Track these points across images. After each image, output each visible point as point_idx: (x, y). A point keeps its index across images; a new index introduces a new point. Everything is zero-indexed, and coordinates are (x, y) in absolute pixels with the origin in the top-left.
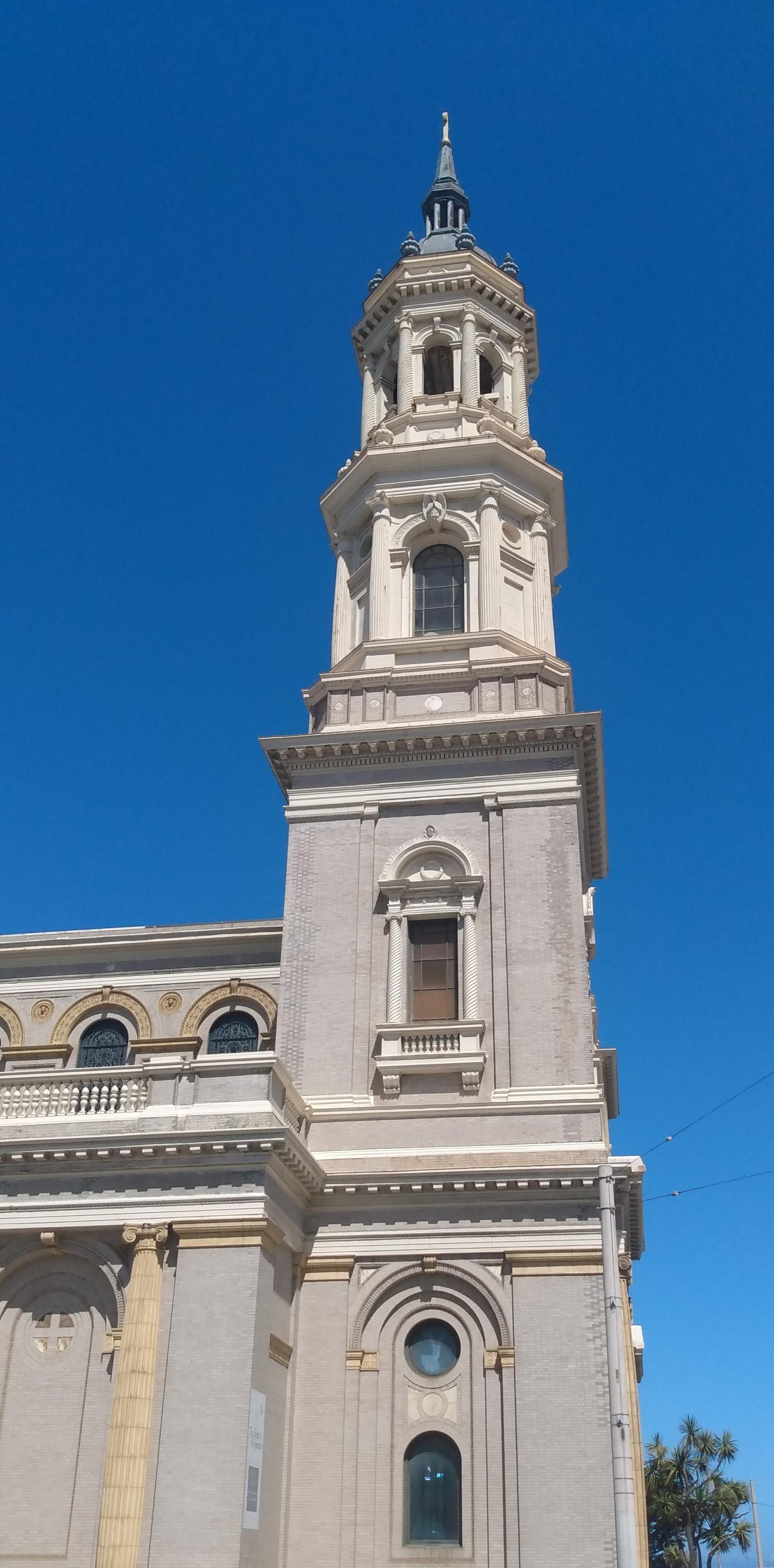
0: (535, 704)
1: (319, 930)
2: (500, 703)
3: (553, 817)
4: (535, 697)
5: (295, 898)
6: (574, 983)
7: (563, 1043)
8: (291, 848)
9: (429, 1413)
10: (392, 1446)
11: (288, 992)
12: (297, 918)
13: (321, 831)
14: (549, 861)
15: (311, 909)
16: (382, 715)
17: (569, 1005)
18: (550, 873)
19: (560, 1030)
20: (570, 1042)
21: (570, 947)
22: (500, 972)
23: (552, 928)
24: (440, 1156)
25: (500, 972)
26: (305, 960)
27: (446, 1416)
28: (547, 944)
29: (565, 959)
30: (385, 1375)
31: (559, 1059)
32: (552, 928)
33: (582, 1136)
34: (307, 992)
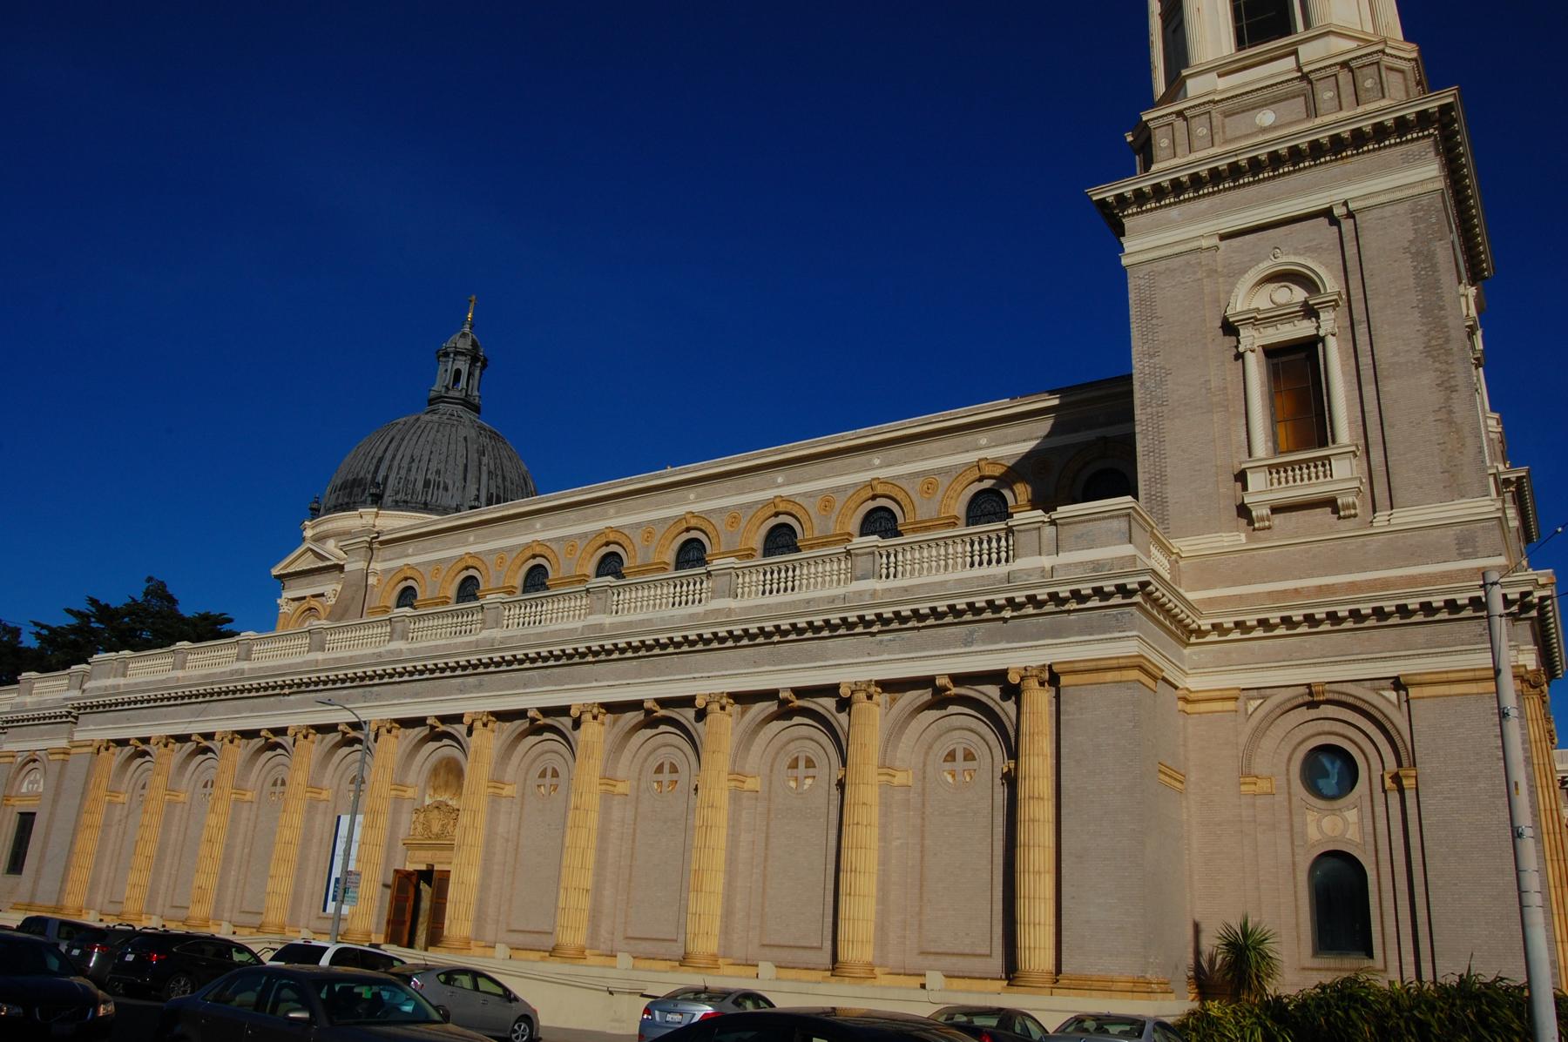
0: (1380, 95)
1: (1170, 374)
2: (1340, 102)
3: (1413, 215)
4: (1379, 86)
6: (1456, 391)
7: (1450, 456)
8: (1132, 296)
9: (1330, 834)
10: (1294, 864)
11: (1145, 440)
13: (1160, 273)
14: (1415, 263)
16: (1210, 143)
17: (1453, 415)
18: (1417, 276)
19: (1444, 443)
20: (1457, 454)
21: (1448, 352)
22: (1369, 391)
23: (1426, 335)
24: (1320, 586)
25: (1369, 391)
26: (1159, 406)
27: (1347, 836)
28: (1421, 353)
29: (1444, 367)
30: (1281, 798)
31: (1446, 474)
32: (1426, 335)
33: (1478, 552)
34: (1164, 437)
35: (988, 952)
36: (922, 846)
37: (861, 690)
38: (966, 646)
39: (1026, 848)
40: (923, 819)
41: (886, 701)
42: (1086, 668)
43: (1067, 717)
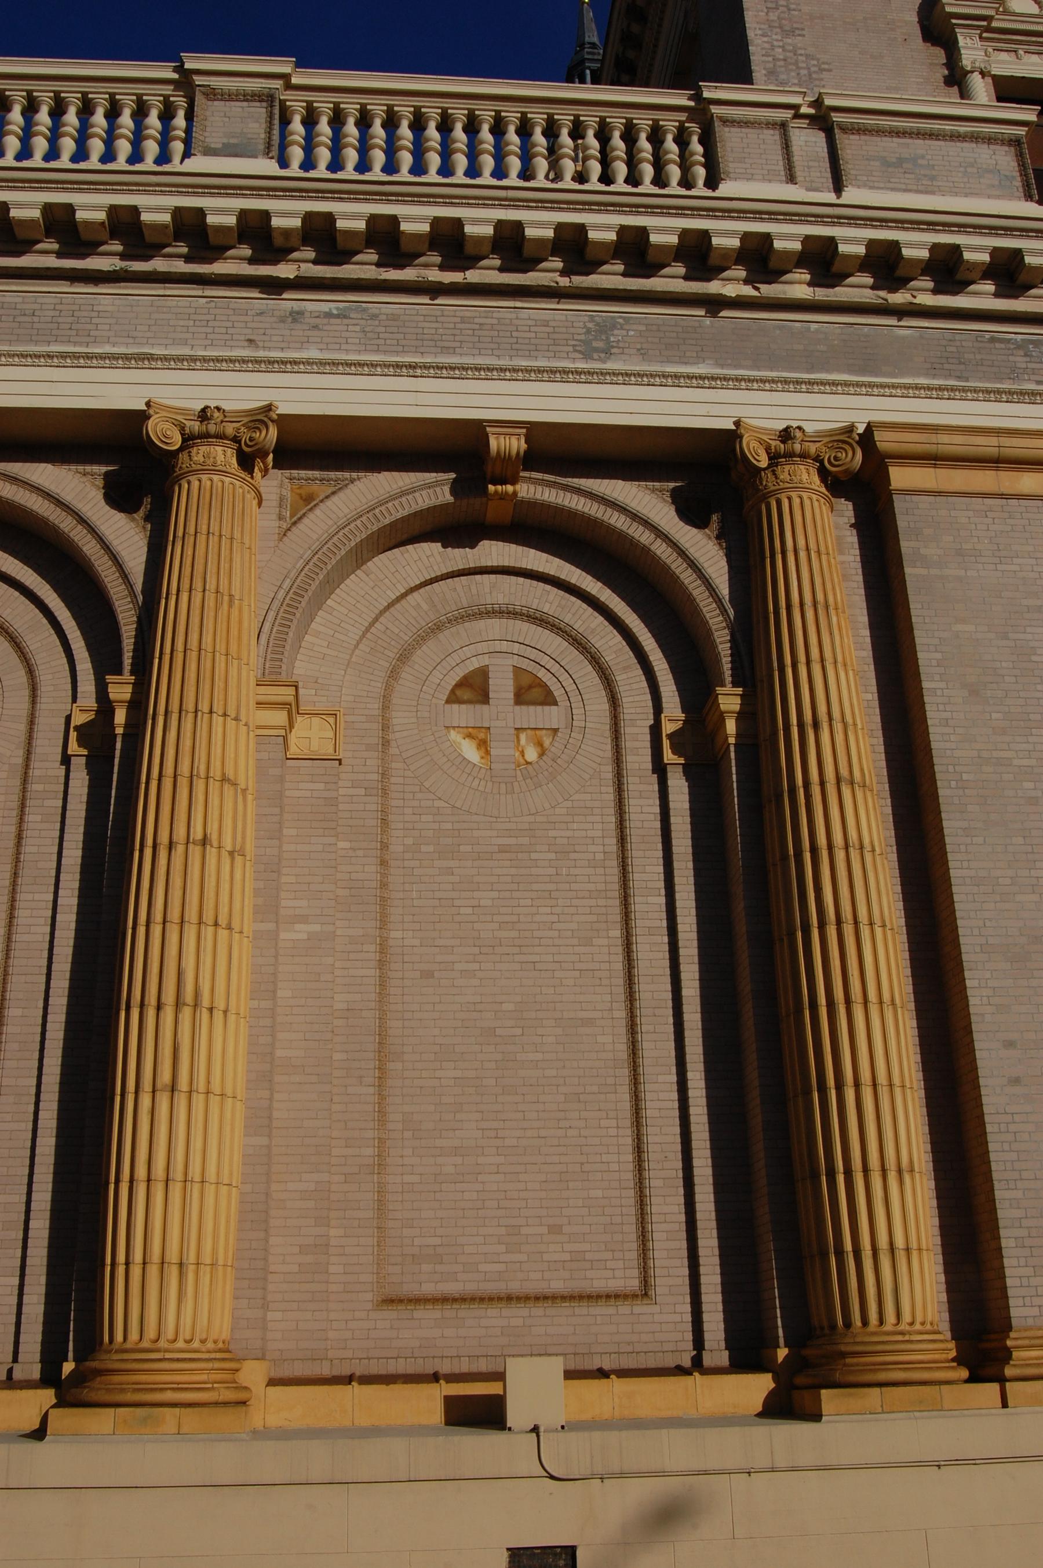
5: (766, 10)
12: (775, 43)
15: (804, 32)
35: (634, 1284)
36: (383, 948)
37: (221, 436)
38: (587, 356)
39: (848, 930)
40: (383, 863)
41: (282, 499)
42: (971, 451)
43: (923, 572)
